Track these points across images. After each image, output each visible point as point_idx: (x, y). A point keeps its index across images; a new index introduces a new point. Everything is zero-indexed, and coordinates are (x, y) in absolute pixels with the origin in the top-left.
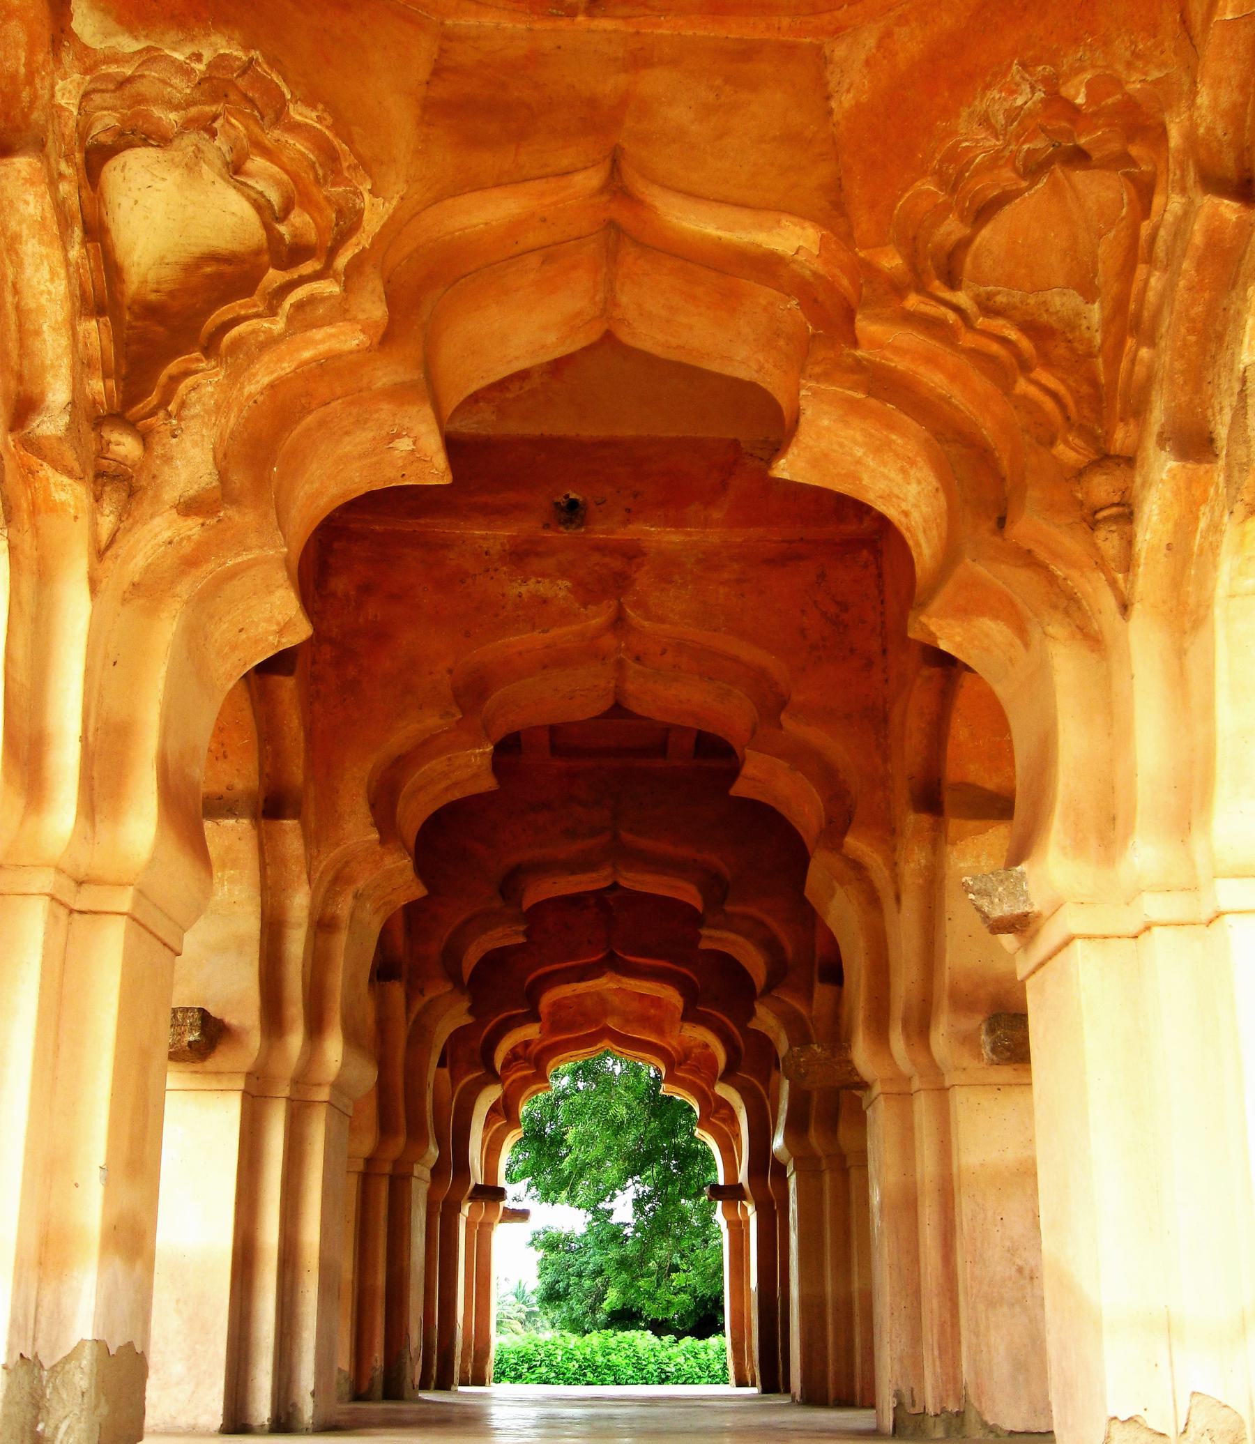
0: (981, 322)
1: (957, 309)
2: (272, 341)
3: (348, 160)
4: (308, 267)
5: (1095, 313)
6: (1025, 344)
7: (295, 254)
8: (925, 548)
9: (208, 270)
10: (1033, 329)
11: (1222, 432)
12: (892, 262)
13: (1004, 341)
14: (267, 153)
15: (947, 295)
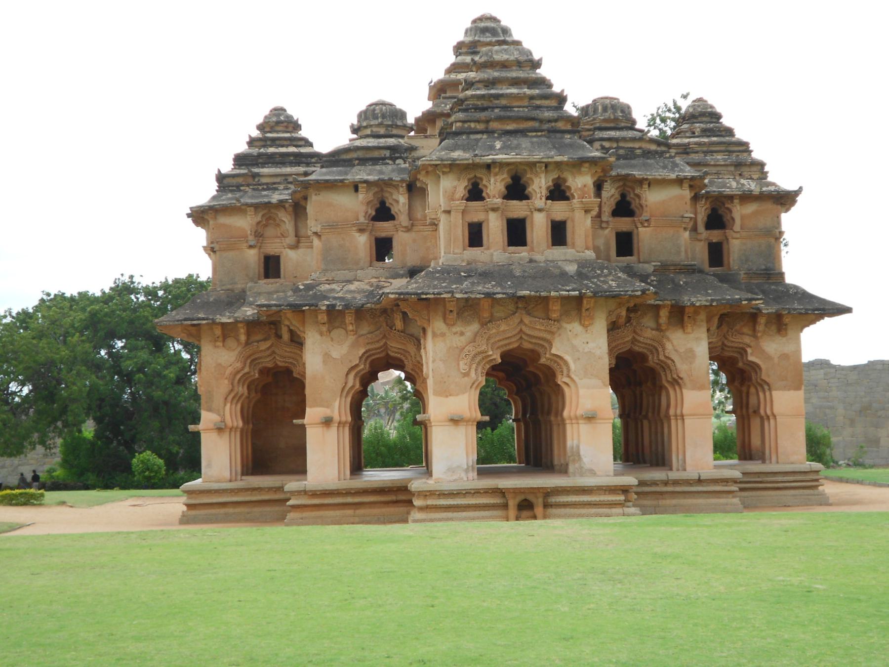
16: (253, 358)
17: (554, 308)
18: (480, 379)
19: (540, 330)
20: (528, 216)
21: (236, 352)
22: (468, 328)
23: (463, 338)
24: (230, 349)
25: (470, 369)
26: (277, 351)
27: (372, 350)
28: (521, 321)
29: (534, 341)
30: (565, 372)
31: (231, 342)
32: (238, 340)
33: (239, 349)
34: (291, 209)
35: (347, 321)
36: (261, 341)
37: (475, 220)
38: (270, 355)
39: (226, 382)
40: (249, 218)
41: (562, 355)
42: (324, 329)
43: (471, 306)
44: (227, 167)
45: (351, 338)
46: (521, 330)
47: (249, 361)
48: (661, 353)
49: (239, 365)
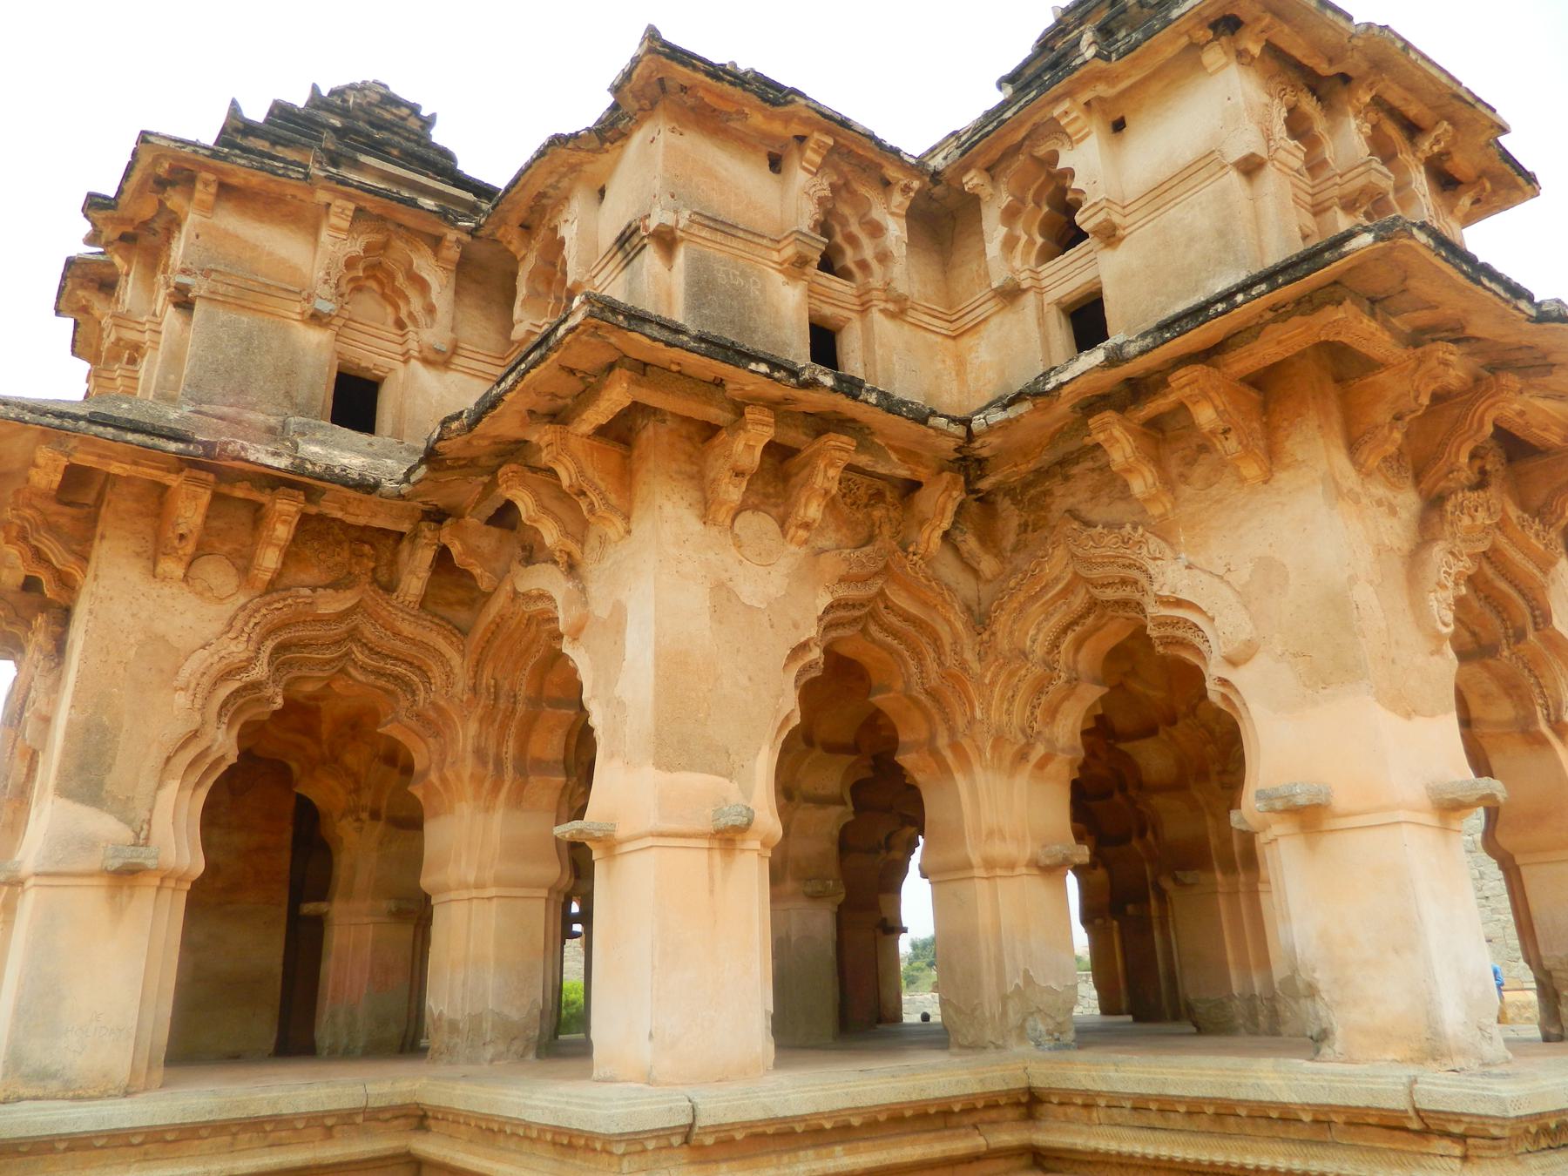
16: (284, 636)
21: (230, 608)
24: (206, 593)
26: (369, 631)
31: (217, 574)
32: (244, 566)
33: (242, 600)
34: (453, 253)
35: (819, 481)
36: (325, 587)
38: (337, 643)
39: (181, 699)
40: (325, 235)
42: (734, 493)
44: (257, 112)
45: (791, 554)
47: (270, 645)
49: (238, 649)
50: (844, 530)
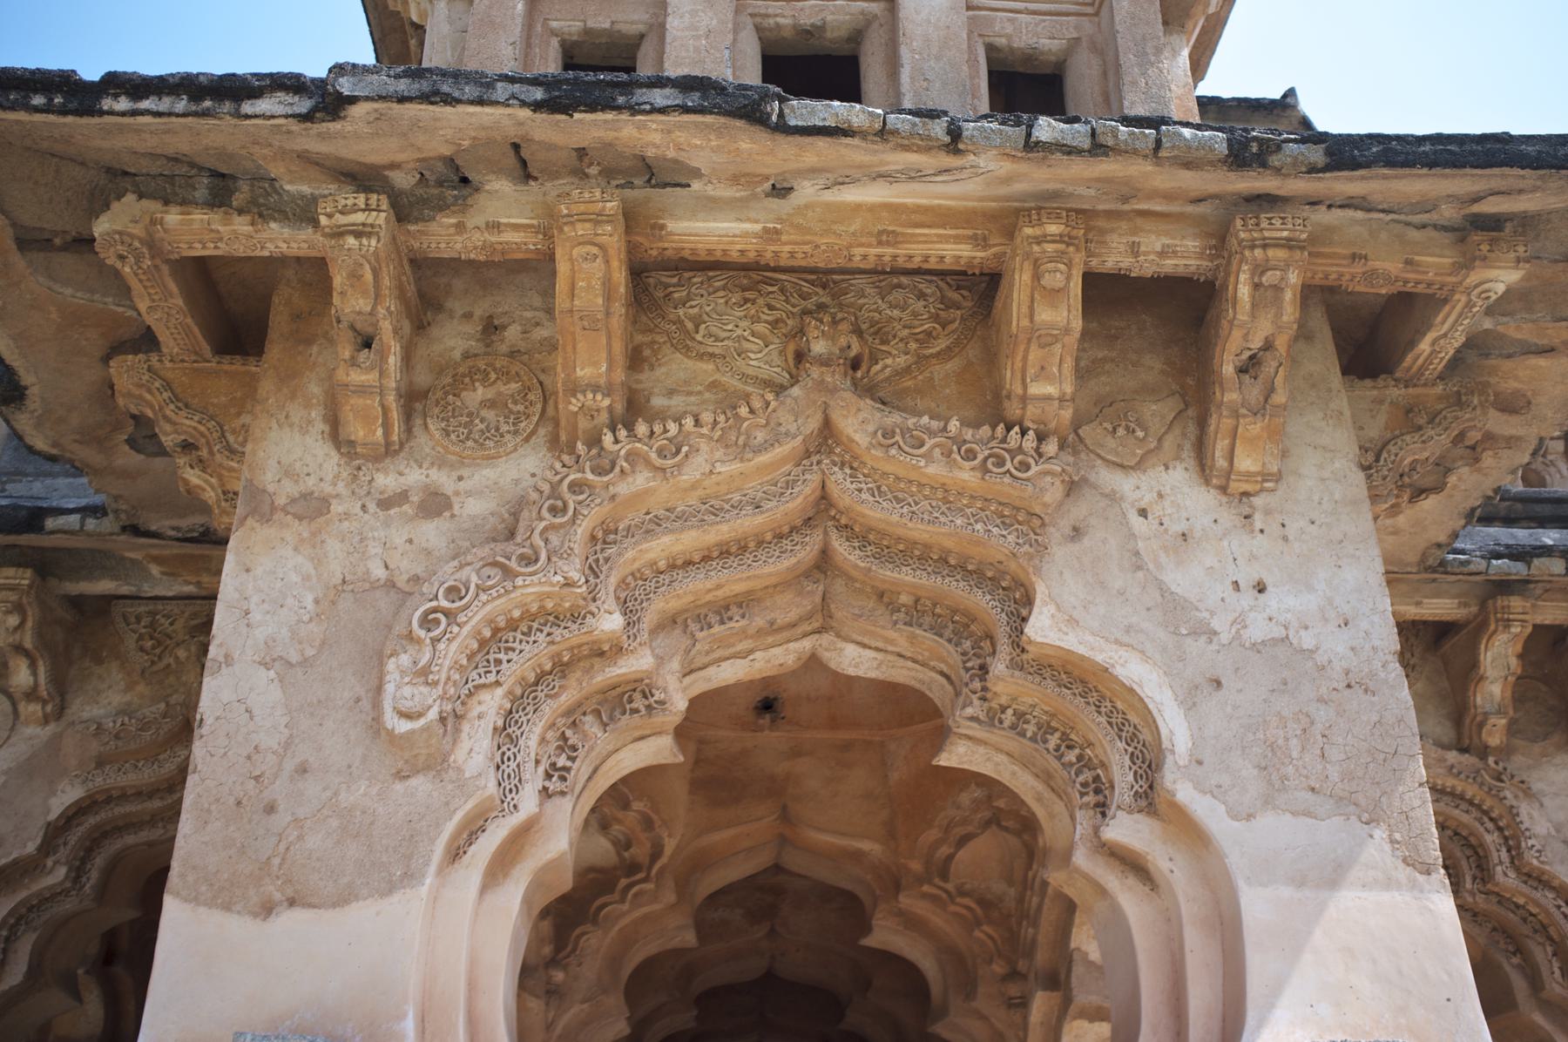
0: (958, 900)
1: (946, 891)
2: (623, 914)
3: (658, 823)
4: (641, 875)
5: (1012, 892)
6: (979, 911)
7: (632, 868)
8: (936, 990)
9: (591, 876)
10: (982, 902)
11: (1063, 977)
12: (916, 866)
13: (968, 908)
14: (619, 821)
15: (941, 884)
17: (1045, 315)
18: (528, 801)
19: (947, 496)
20: (869, 20)
22: (486, 475)
23: (433, 533)
25: (452, 721)
27: (123, 797)
28: (827, 437)
29: (907, 578)
30: (1123, 778)
37: (601, 22)
41: (1099, 651)
43: (513, 354)
46: (823, 506)
48: (1499, 855)
50: (141, 688)
